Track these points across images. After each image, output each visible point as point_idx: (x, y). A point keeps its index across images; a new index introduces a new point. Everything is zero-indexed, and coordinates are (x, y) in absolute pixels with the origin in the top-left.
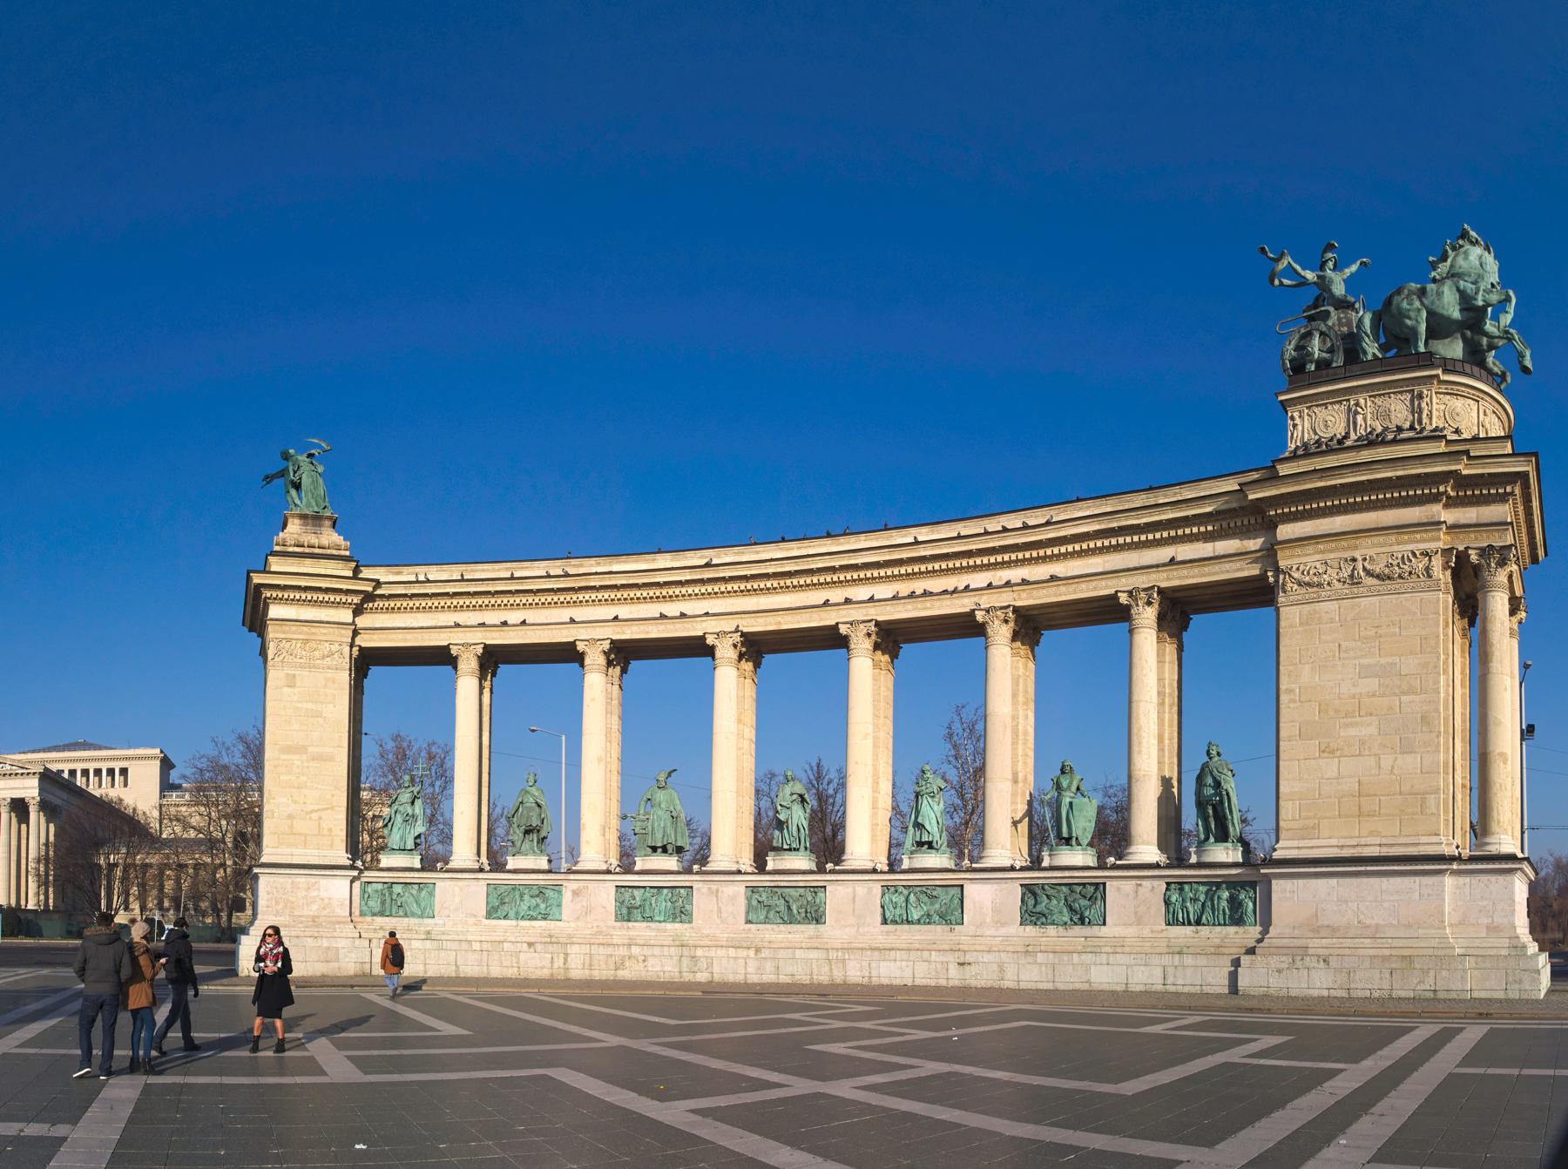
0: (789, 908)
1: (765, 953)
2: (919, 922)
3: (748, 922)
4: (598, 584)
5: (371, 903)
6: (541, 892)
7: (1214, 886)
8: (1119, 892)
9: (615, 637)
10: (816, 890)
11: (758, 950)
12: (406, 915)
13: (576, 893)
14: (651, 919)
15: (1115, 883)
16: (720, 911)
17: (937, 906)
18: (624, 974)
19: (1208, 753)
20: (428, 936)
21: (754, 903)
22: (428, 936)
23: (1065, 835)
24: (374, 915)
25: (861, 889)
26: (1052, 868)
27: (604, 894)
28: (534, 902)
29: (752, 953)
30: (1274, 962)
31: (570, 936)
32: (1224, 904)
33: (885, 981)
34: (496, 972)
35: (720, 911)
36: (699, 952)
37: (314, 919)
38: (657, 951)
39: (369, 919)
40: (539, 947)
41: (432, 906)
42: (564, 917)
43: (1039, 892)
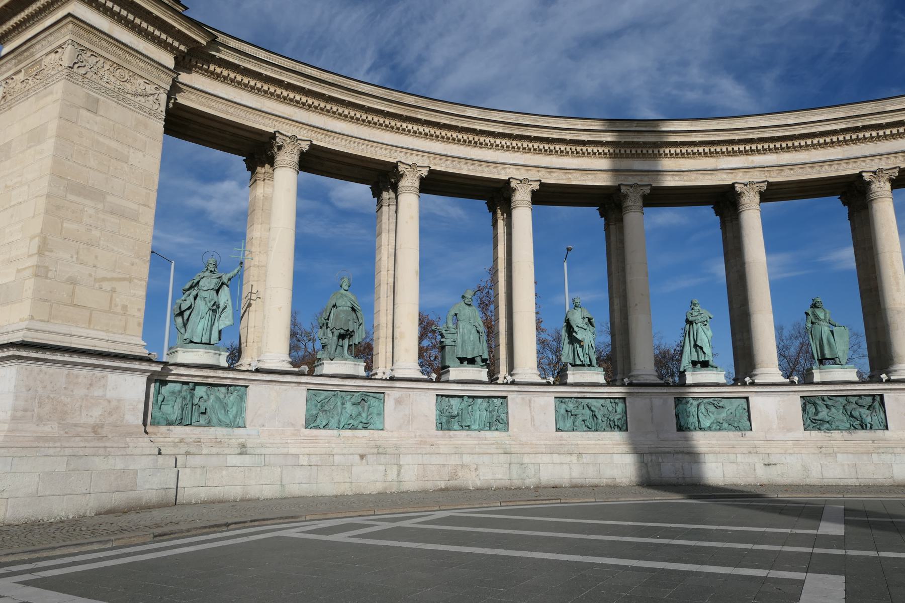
1: (586, 459)
2: (710, 428)
3: (558, 430)
4: (424, 118)
5: (166, 409)
6: (364, 398)
9: (433, 168)
12: (209, 424)
13: (398, 402)
15: (892, 394)
16: (533, 419)
17: (724, 415)
20: (243, 450)
21: (563, 411)
22: (243, 450)
23: (828, 355)
24: (169, 423)
25: (657, 402)
26: (818, 384)
27: (425, 402)
29: (574, 458)
35: (533, 419)
36: (526, 459)
39: (163, 429)
40: (371, 459)
41: (240, 413)
42: (387, 425)
43: (820, 402)
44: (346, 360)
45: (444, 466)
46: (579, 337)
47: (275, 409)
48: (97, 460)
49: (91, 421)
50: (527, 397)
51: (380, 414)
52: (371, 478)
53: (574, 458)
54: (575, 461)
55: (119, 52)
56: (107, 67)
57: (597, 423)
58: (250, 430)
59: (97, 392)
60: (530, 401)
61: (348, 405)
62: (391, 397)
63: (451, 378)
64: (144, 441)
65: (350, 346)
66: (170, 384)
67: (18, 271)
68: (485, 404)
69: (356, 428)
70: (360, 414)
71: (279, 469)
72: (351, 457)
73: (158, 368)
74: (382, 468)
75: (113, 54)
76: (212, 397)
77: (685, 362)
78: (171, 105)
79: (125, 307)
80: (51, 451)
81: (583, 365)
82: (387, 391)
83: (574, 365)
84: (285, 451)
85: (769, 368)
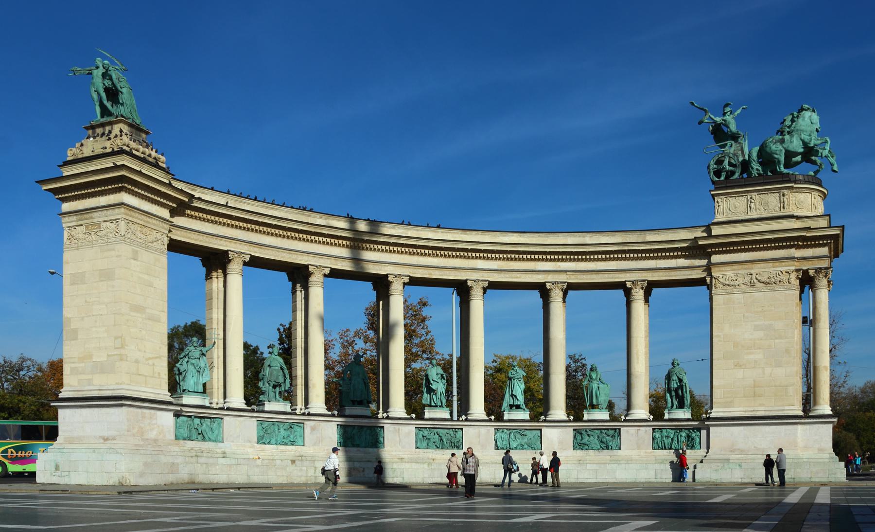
0: (441, 440)
2: (516, 448)
3: (417, 448)
7: (678, 429)
8: (628, 433)
10: (455, 430)
12: (204, 439)
13: (313, 429)
14: (358, 446)
17: (526, 440)
19: (673, 364)
20: (224, 455)
21: (421, 436)
22: (224, 455)
23: (595, 402)
24: (184, 439)
25: (483, 430)
29: (426, 466)
30: (713, 466)
32: (683, 439)
37: (155, 441)
39: (182, 442)
43: (584, 433)
44: (279, 401)
46: (434, 387)
47: (240, 430)
48: (162, 457)
50: (397, 427)
51: (303, 436)
53: (426, 466)
57: (443, 444)
61: (282, 430)
62: (308, 425)
64: (176, 449)
65: (280, 392)
66: (181, 418)
67: (108, 355)
68: (369, 431)
69: (286, 444)
70: (289, 436)
73: (178, 408)
74: (304, 468)
76: (204, 425)
77: (505, 405)
79: (159, 374)
80: (142, 452)
81: (436, 406)
82: (305, 422)
83: (430, 406)
84: (245, 456)
85: (559, 409)
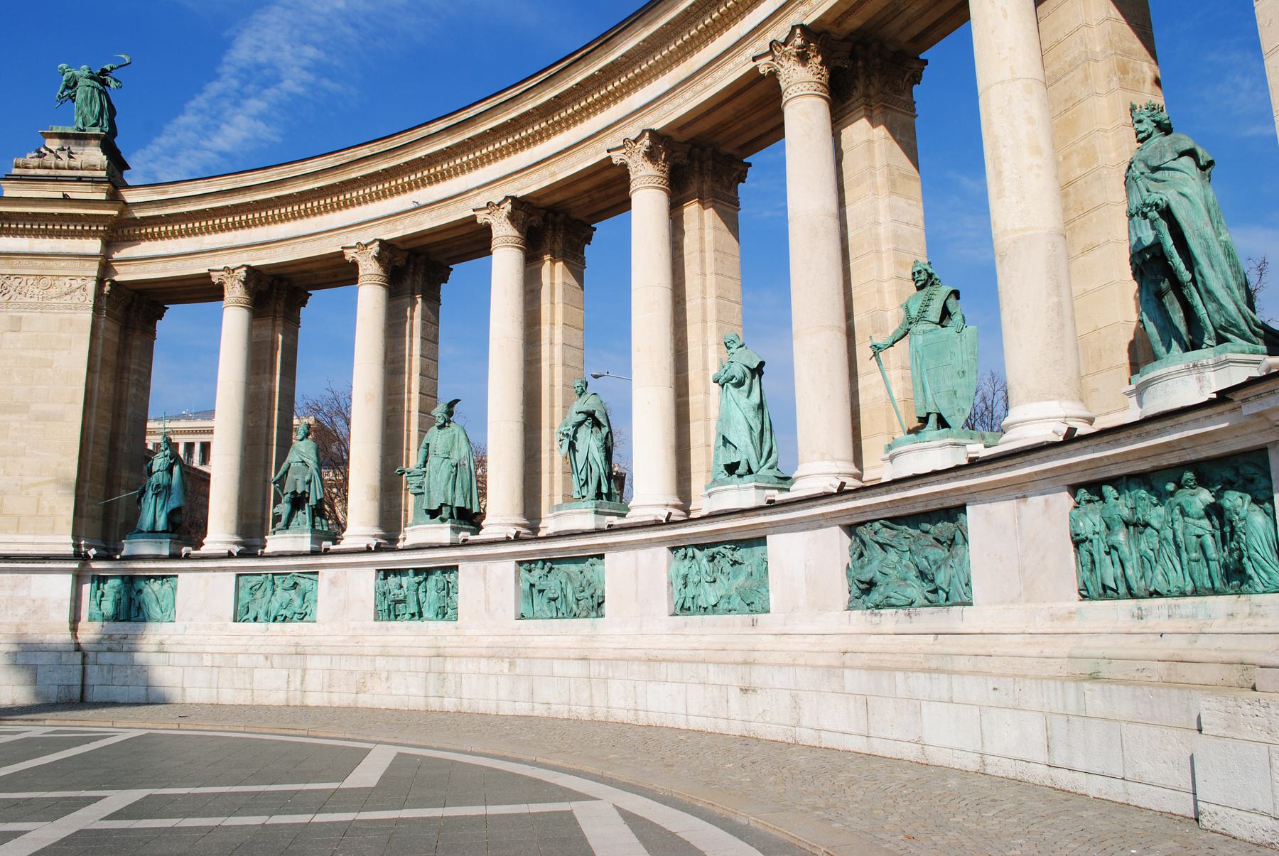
1: (521, 666)
11: (512, 664)
13: (333, 582)
16: (487, 602)
18: (366, 700)
28: (287, 595)
31: (318, 645)
33: (654, 719)
34: (229, 696)
35: (487, 602)
38: (402, 663)
45: (352, 672)
49: (17, 620)
52: (272, 688)
54: (506, 671)
55: (39, 263)
56: (30, 282)
58: (178, 625)
59: (21, 593)
60: (485, 570)
63: (268, 550)
71: (181, 670)
72: (255, 657)
75: (34, 268)
78: (107, 288)
